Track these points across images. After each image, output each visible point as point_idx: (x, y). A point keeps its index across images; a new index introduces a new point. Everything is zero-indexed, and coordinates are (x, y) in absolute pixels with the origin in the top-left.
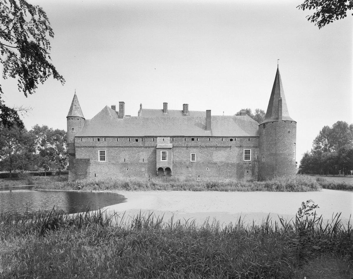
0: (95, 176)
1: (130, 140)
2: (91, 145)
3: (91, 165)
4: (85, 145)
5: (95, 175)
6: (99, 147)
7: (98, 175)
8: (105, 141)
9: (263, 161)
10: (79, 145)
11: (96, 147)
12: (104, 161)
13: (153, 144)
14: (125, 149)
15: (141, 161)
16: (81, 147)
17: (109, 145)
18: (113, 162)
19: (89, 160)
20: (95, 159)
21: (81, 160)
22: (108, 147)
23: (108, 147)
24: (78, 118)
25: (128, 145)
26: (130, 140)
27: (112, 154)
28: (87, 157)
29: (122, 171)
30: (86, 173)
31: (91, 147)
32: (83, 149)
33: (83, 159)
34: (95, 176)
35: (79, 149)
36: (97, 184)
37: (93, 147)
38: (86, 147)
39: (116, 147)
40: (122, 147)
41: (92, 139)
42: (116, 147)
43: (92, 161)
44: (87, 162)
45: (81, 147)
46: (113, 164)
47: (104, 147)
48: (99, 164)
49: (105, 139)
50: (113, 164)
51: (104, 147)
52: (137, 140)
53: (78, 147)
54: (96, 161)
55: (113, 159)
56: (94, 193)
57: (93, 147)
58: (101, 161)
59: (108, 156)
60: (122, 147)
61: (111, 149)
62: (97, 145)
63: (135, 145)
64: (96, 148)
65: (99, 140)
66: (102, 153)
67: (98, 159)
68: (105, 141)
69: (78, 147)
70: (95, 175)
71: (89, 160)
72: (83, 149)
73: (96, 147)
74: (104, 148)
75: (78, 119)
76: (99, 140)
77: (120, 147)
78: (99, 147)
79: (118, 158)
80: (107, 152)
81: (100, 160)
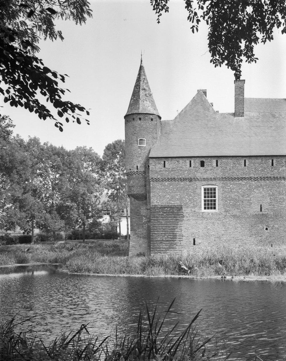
0: (194, 244)
1: (272, 165)
2: (186, 175)
4: (173, 176)
6: (204, 179)
7: (200, 241)
8: (217, 165)
10: (159, 177)
11: (196, 179)
12: (213, 211)
14: (263, 183)
16: (163, 180)
17: (227, 175)
18: (236, 212)
20: (195, 207)
21: (163, 208)
22: (223, 179)
23: (223, 179)
24: (151, 116)
25: (269, 175)
26: (272, 165)
27: (233, 195)
28: (177, 203)
29: (254, 231)
30: (175, 236)
31: (185, 179)
32: (166, 184)
33: (168, 207)
34: (194, 244)
36: (221, 262)
37: (191, 180)
39: (242, 179)
41: (188, 162)
42: (242, 179)
43: (186, 211)
45: (163, 180)
46: (234, 216)
47: (215, 179)
48: (203, 217)
49: (217, 162)
50: (234, 216)
51: (215, 179)
53: (157, 180)
54: (196, 209)
55: (234, 206)
56: (231, 282)
57: (191, 180)
58: (207, 211)
59: (225, 199)
60: (256, 179)
61: (231, 185)
62: (198, 175)
64: (197, 183)
65: (202, 164)
66: (210, 193)
67: (201, 207)
68: (217, 165)
69: (157, 180)
71: (180, 208)
72: (166, 184)
73: (196, 179)
74: (214, 182)
75: (152, 120)
76: (202, 164)
77: (250, 178)
78: (204, 179)
79: (245, 202)
80: (222, 190)
81: (205, 208)
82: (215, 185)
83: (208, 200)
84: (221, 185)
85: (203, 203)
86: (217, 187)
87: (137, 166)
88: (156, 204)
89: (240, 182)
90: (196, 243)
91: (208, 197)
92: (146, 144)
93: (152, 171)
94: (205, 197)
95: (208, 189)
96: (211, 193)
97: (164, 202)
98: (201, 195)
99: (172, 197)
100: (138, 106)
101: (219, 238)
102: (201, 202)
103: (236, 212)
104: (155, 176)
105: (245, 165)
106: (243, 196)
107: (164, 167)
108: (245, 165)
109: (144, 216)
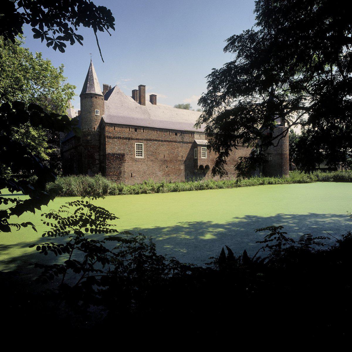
0: (132, 177)
2: (126, 136)
3: (126, 161)
4: (120, 136)
5: (132, 175)
6: (137, 139)
7: (135, 175)
9: (270, 159)
10: (111, 135)
11: (133, 139)
12: (141, 157)
13: (191, 140)
15: (180, 158)
19: (123, 155)
20: (132, 155)
21: (114, 154)
22: (147, 140)
23: (147, 140)
24: (102, 97)
25: (168, 139)
27: (151, 149)
29: (161, 169)
30: (120, 173)
31: (126, 138)
33: (117, 154)
34: (132, 177)
35: (111, 141)
37: (129, 139)
38: (120, 138)
40: (162, 141)
43: (127, 157)
44: (121, 158)
46: (152, 160)
47: (142, 139)
48: (136, 161)
50: (152, 160)
52: (176, 134)
53: (110, 138)
55: (152, 155)
57: (129, 139)
58: (138, 157)
60: (162, 141)
61: (150, 143)
62: (134, 137)
63: (174, 140)
66: (140, 147)
67: (135, 155)
69: (110, 138)
70: (132, 175)
71: (123, 155)
74: (141, 141)
78: (137, 139)
81: (137, 156)
82: (142, 143)
83: (138, 151)
84: (145, 143)
85: (136, 152)
86: (143, 144)
87: (94, 127)
88: (109, 152)
89: (154, 142)
90: (132, 176)
91: (138, 149)
92: (100, 114)
93: (107, 131)
94: (137, 149)
95: (138, 145)
96: (140, 147)
97: (114, 151)
98: (135, 148)
99: (119, 149)
100: (94, 89)
101: (145, 173)
102: (135, 152)
103: (153, 158)
104: (109, 135)
105: (157, 133)
106: (156, 150)
107: (115, 129)
108: (157, 133)
109: (97, 159)
